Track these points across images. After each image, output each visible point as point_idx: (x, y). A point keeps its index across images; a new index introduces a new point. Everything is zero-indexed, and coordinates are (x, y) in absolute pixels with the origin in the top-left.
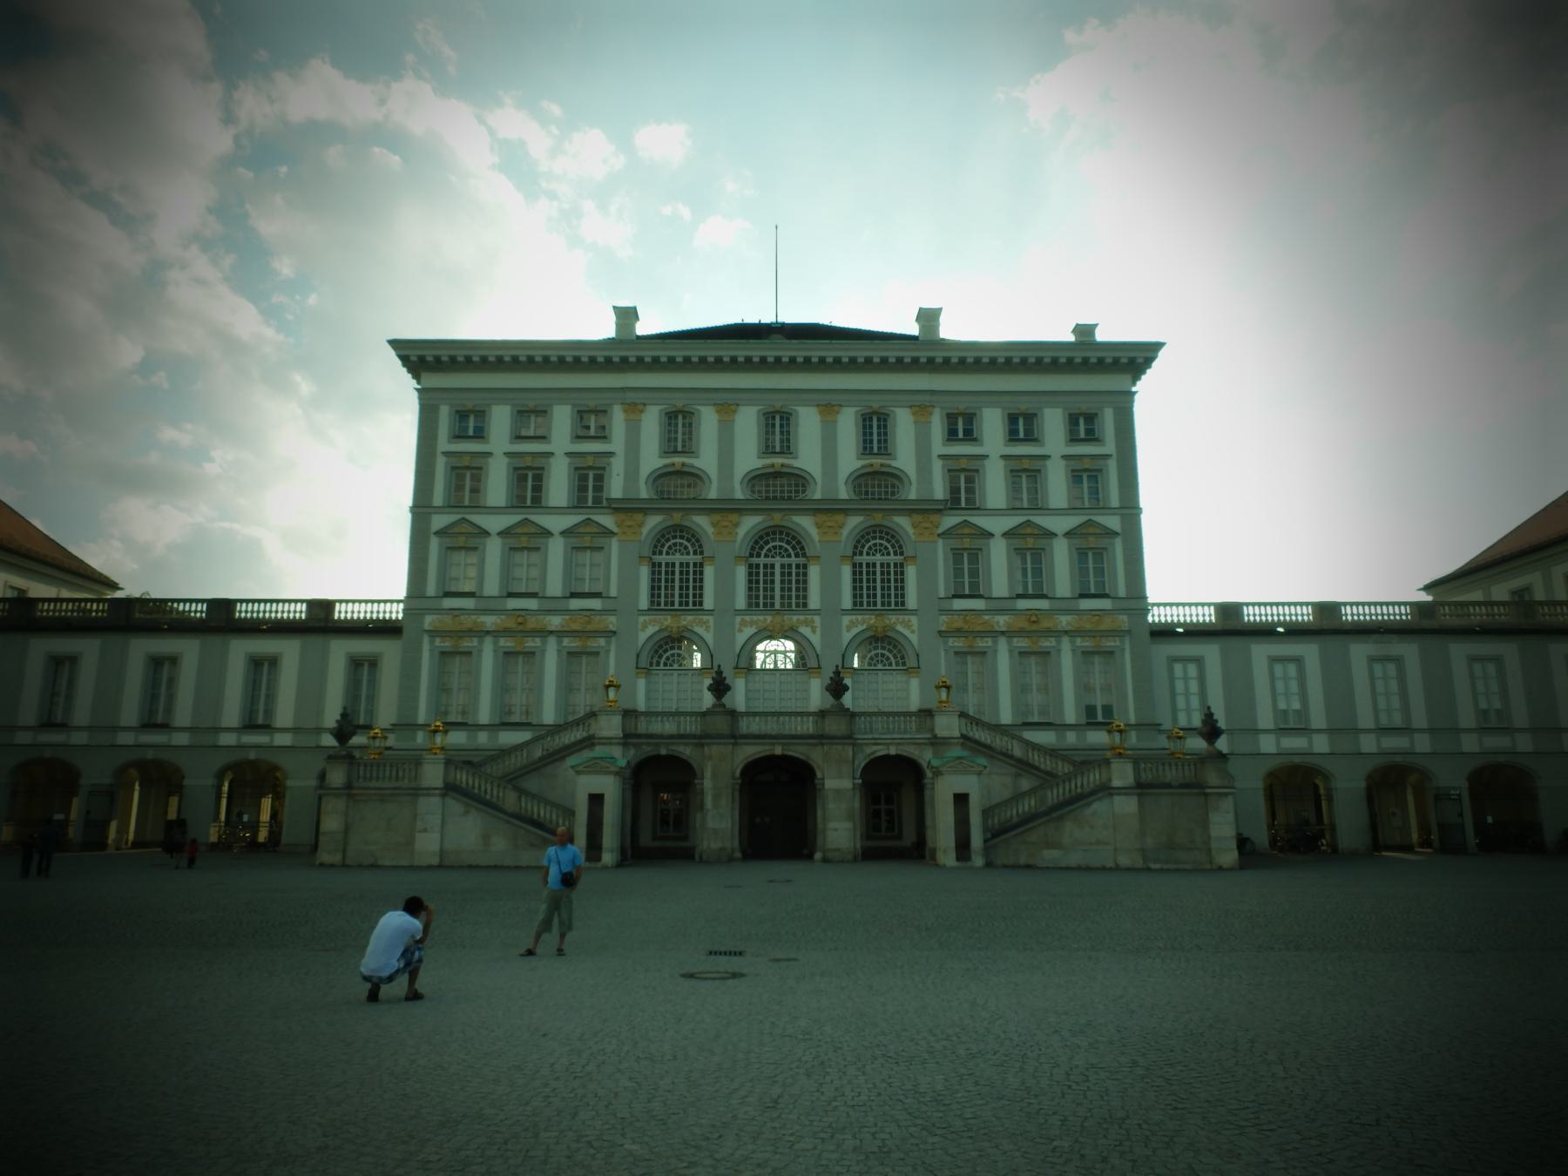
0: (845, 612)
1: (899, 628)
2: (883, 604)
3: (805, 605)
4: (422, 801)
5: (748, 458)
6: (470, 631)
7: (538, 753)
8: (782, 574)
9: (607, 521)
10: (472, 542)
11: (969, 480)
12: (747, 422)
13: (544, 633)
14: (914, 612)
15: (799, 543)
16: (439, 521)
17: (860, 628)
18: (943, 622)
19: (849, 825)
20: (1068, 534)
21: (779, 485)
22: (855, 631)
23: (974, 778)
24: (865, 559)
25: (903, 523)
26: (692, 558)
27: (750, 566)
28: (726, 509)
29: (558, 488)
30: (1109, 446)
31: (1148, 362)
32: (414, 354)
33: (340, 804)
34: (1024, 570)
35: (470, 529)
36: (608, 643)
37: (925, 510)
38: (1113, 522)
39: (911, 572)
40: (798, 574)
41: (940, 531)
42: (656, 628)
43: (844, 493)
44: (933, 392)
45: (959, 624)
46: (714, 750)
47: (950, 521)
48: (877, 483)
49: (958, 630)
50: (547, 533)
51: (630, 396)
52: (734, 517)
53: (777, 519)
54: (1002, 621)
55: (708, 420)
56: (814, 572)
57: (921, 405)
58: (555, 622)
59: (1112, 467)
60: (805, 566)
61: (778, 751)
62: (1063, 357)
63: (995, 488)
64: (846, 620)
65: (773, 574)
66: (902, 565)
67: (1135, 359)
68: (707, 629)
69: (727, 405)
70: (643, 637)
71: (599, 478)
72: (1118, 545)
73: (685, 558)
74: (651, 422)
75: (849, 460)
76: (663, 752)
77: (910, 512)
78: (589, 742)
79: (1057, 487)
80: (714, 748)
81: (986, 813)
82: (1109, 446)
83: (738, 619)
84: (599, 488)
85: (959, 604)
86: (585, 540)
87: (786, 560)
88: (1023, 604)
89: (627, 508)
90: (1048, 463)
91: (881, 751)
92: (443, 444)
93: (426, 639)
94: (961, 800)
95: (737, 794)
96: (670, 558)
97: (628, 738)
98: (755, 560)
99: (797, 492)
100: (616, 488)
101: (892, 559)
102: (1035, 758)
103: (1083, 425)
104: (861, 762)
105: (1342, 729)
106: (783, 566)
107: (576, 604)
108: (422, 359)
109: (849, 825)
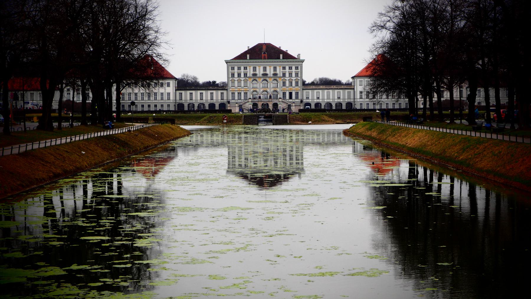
5: (262, 72)
16: (230, 79)
21: (265, 75)
28: (260, 77)
29: (242, 75)
30: (299, 70)
37: (280, 77)
43: (272, 76)
48: (275, 75)
57: (280, 66)
63: (287, 75)
69: (259, 66)
74: (252, 68)
75: (272, 72)
79: (294, 75)
82: (299, 70)
86: (245, 81)
89: (249, 77)
92: (230, 71)
100: (248, 75)
103: (297, 68)
105: (323, 99)
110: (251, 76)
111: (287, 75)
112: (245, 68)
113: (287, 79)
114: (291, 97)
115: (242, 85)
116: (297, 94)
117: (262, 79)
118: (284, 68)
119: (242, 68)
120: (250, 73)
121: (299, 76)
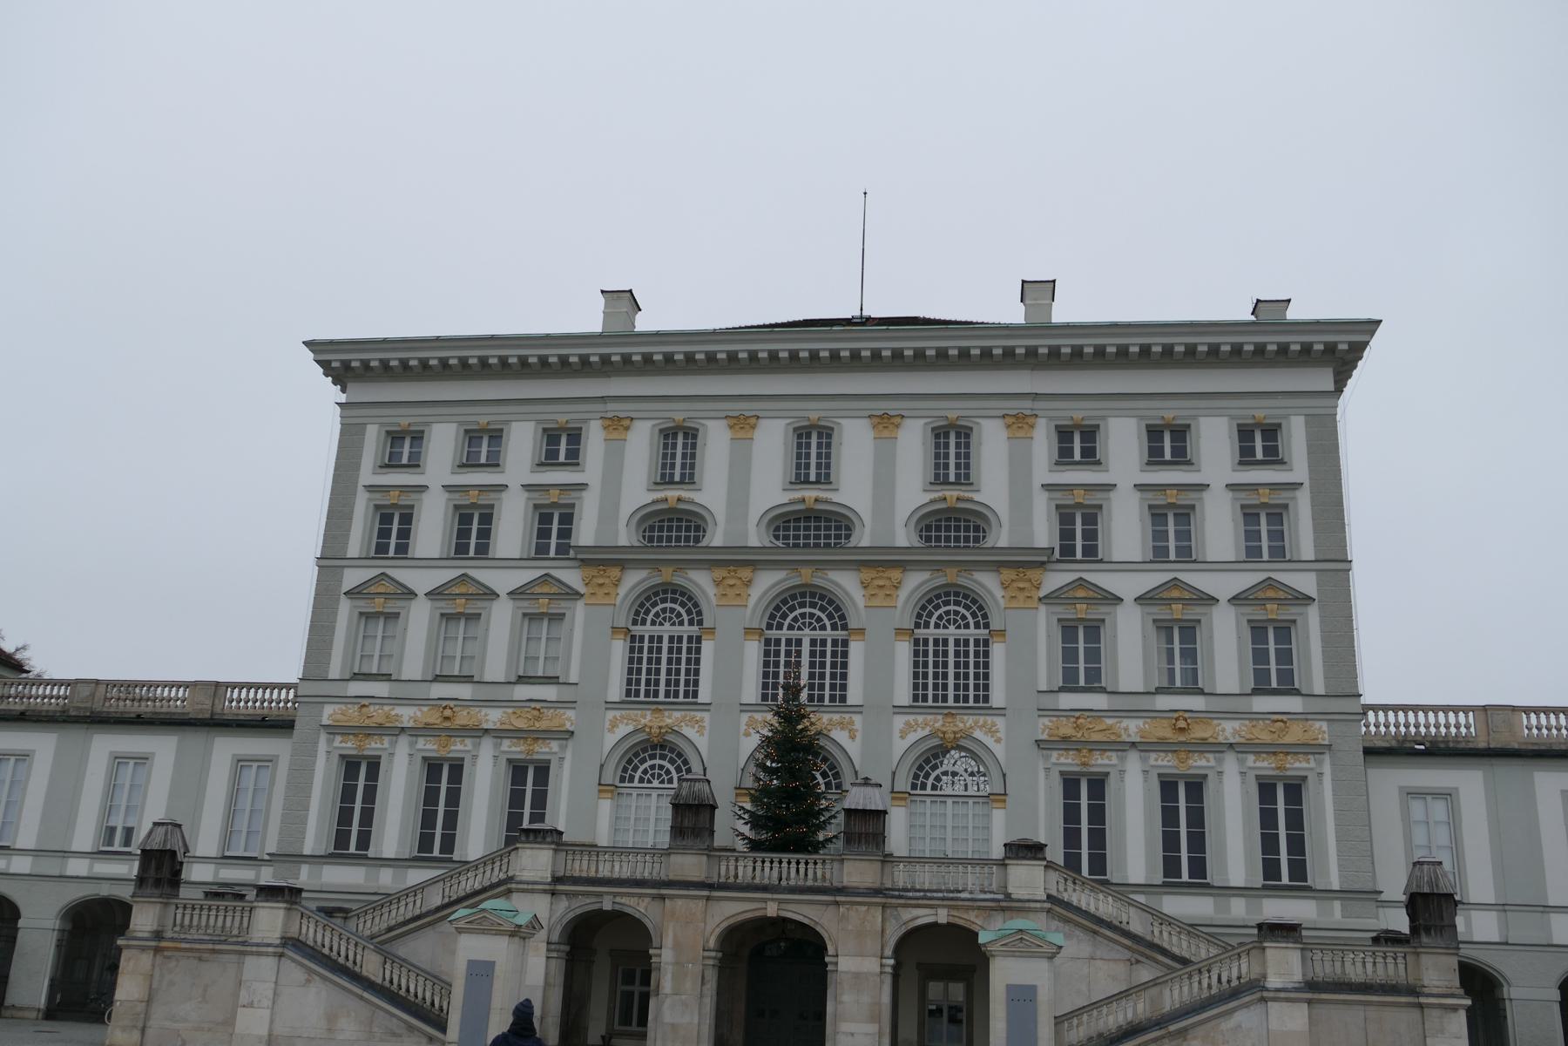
0: (899, 709)
1: (978, 734)
2: (957, 699)
3: (843, 699)
4: (250, 961)
6: (381, 726)
7: (436, 900)
8: (813, 654)
9: (572, 577)
10: (391, 607)
11: (1091, 519)
12: (772, 443)
13: (478, 732)
14: (1001, 711)
15: (838, 609)
17: (921, 733)
18: (1043, 727)
19: (873, 1028)
20: (1236, 600)
21: (812, 528)
22: (912, 737)
23: (1043, 965)
24: (931, 632)
25: (988, 584)
26: (686, 630)
27: (768, 642)
28: (736, 562)
29: (512, 530)
30: (1299, 470)
31: (1358, 350)
32: (335, 359)
33: (146, 959)
34: (1170, 652)
35: (391, 589)
36: (563, 748)
37: (1023, 563)
38: (1305, 583)
39: (997, 651)
40: (834, 654)
41: (1042, 593)
42: (630, 728)
44: (1036, 396)
45: (1067, 729)
46: (683, 905)
47: (1055, 580)
48: (952, 525)
49: (1065, 739)
50: (492, 595)
51: (614, 408)
52: (745, 573)
53: (806, 576)
54: (1132, 728)
55: (716, 441)
56: (856, 650)
58: (493, 717)
59: (1303, 506)
60: (845, 643)
61: (772, 910)
62: (1226, 342)
63: (1126, 530)
64: (899, 721)
65: (799, 654)
66: (986, 643)
67: (1338, 349)
68: (700, 732)
70: (611, 739)
71: (567, 519)
72: (1313, 615)
73: (677, 630)
74: (641, 443)
75: (913, 491)
76: (607, 905)
77: (998, 566)
78: (505, 887)
79: (1219, 529)
80: (679, 902)
81: (1059, 1021)
82: (1299, 470)
83: (745, 717)
84: (565, 533)
85: (1068, 701)
86: (543, 608)
87: (818, 634)
88: (1164, 702)
89: (602, 561)
90: (1205, 495)
91: (924, 916)
92: (367, 474)
93: (323, 737)
94: (1023, 997)
95: (712, 976)
96: (657, 630)
97: (558, 884)
98: (773, 634)
99: (838, 537)
100: (586, 533)
101: (972, 632)
102: (1167, 939)
103: (1258, 441)
104: (894, 934)
106: (813, 642)
107: (523, 692)
108: (346, 365)
109: (873, 1028)
110: (625, 537)
111: (1126, 530)
112: (562, 444)
113: (1129, 586)
114: (1185, 852)
115: (496, 666)
116: (1280, 804)
117: (766, 583)
118: (1077, 443)
119: (522, 441)
120: (608, 515)
121: (1304, 542)
